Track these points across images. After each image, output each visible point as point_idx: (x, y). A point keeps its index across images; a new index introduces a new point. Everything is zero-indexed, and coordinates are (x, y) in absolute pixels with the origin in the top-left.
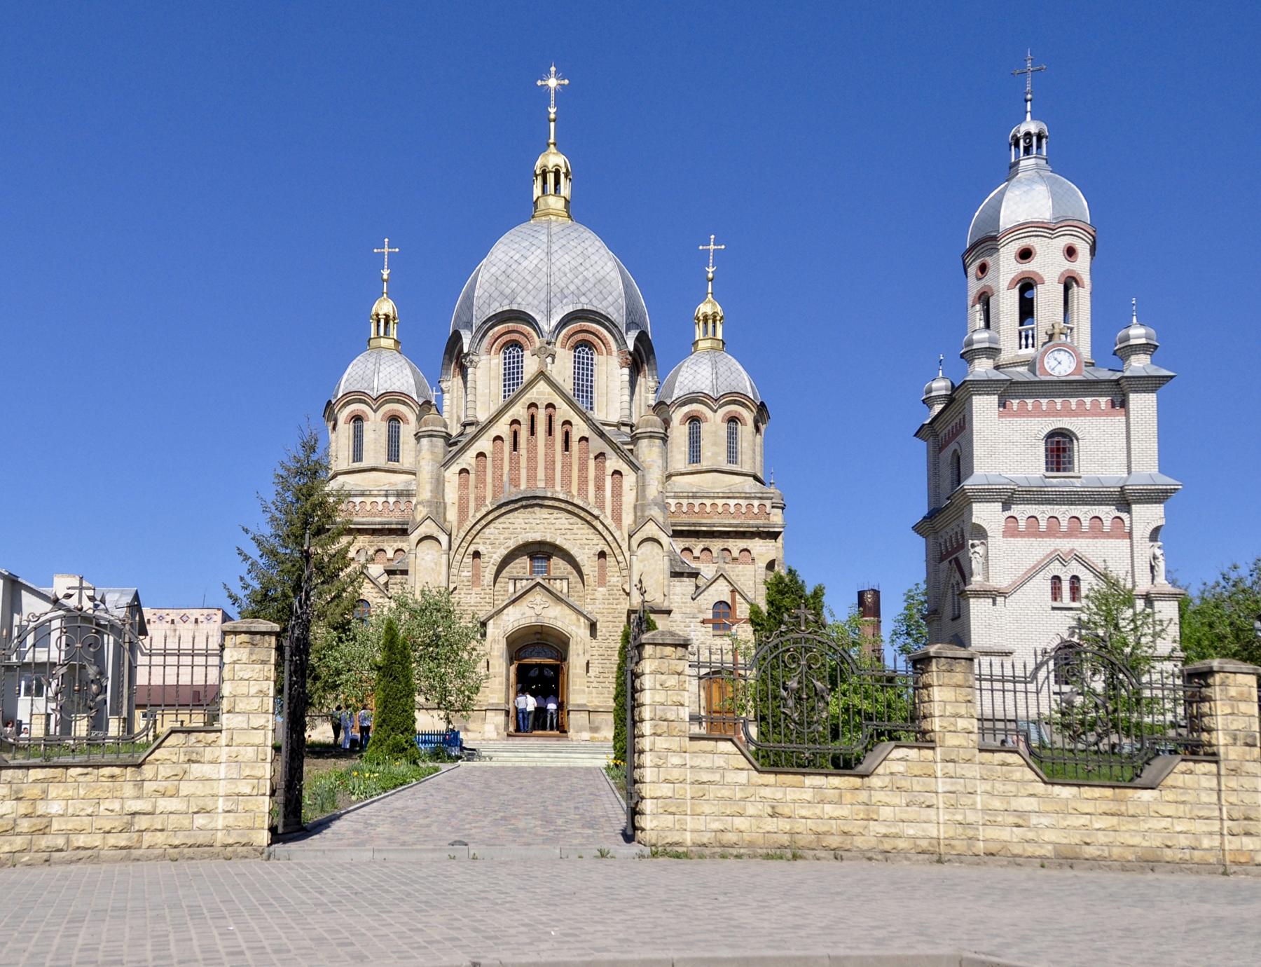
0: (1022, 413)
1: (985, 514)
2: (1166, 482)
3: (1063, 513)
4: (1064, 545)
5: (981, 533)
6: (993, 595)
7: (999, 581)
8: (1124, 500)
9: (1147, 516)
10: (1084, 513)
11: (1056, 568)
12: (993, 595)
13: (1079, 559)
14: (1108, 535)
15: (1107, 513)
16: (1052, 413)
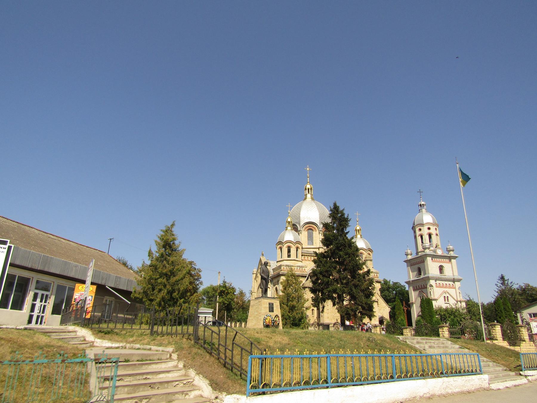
0: (435, 261)
1: (432, 282)
2: (460, 277)
3: (444, 283)
4: (446, 290)
5: (431, 286)
6: (436, 300)
7: (436, 297)
8: (454, 281)
9: (457, 284)
10: (448, 283)
11: (444, 295)
12: (436, 300)
13: (448, 293)
14: (451, 288)
15: (451, 283)
16: (439, 262)
